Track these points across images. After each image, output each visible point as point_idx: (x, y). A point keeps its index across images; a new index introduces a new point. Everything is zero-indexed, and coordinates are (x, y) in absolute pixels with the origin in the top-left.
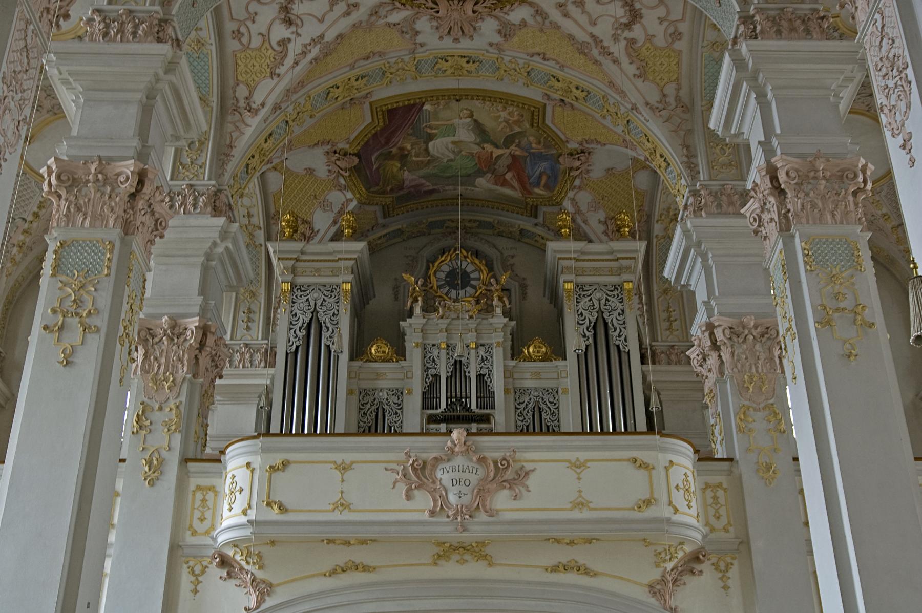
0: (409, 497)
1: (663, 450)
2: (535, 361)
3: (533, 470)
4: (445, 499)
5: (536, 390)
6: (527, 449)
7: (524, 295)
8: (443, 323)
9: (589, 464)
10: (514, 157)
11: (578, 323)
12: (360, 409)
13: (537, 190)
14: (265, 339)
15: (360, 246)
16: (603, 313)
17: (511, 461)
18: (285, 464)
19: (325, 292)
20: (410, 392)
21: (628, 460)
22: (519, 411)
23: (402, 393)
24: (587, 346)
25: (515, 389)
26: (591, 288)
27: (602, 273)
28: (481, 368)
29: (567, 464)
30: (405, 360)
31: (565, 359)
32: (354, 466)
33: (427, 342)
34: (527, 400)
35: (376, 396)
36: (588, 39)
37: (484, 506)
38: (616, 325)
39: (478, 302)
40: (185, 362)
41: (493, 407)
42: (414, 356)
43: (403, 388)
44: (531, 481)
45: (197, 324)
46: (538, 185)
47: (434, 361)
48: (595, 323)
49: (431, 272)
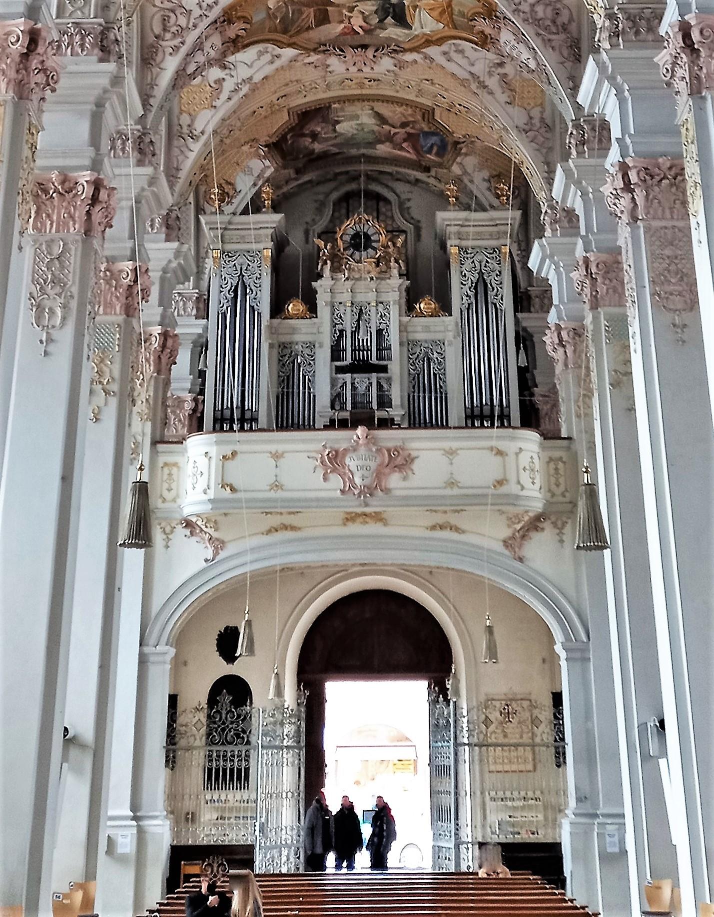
0: (325, 479)
1: (513, 438)
2: (425, 317)
3: (417, 457)
4: (352, 481)
5: (426, 341)
6: (413, 439)
7: (418, 236)
8: (349, 283)
9: (459, 452)
10: (409, 134)
11: (462, 283)
12: (280, 360)
13: (428, 156)
14: (196, 289)
15: (278, 217)
16: (483, 273)
17: (401, 452)
18: (234, 454)
19: (249, 257)
20: (321, 346)
21: (488, 449)
22: (411, 361)
23: (314, 346)
24: (469, 304)
25: (408, 340)
26: (473, 251)
27: (483, 237)
28: (380, 323)
29: (442, 452)
30: (317, 317)
31: (450, 315)
32: (285, 455)
33: (335, 300)
34: (418, 351)
35: (293, 349)
36: (468, 76)
37: (380, 486)
38: (494, 285)
39: (377, 265)
40: (152, 363)
41: (390, 359)
42: (323, 310)
43: (315, 341)
44: (416, 466)
45: (160, 332)
46: (430, 151)
47: (341, 317)
48: (477, 283)
49: (338, 236)
